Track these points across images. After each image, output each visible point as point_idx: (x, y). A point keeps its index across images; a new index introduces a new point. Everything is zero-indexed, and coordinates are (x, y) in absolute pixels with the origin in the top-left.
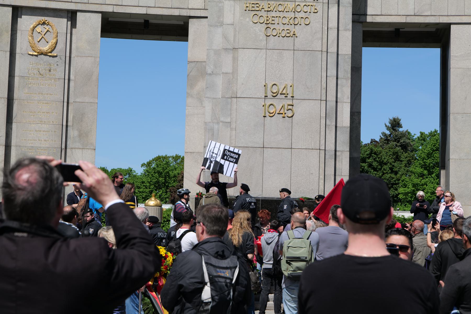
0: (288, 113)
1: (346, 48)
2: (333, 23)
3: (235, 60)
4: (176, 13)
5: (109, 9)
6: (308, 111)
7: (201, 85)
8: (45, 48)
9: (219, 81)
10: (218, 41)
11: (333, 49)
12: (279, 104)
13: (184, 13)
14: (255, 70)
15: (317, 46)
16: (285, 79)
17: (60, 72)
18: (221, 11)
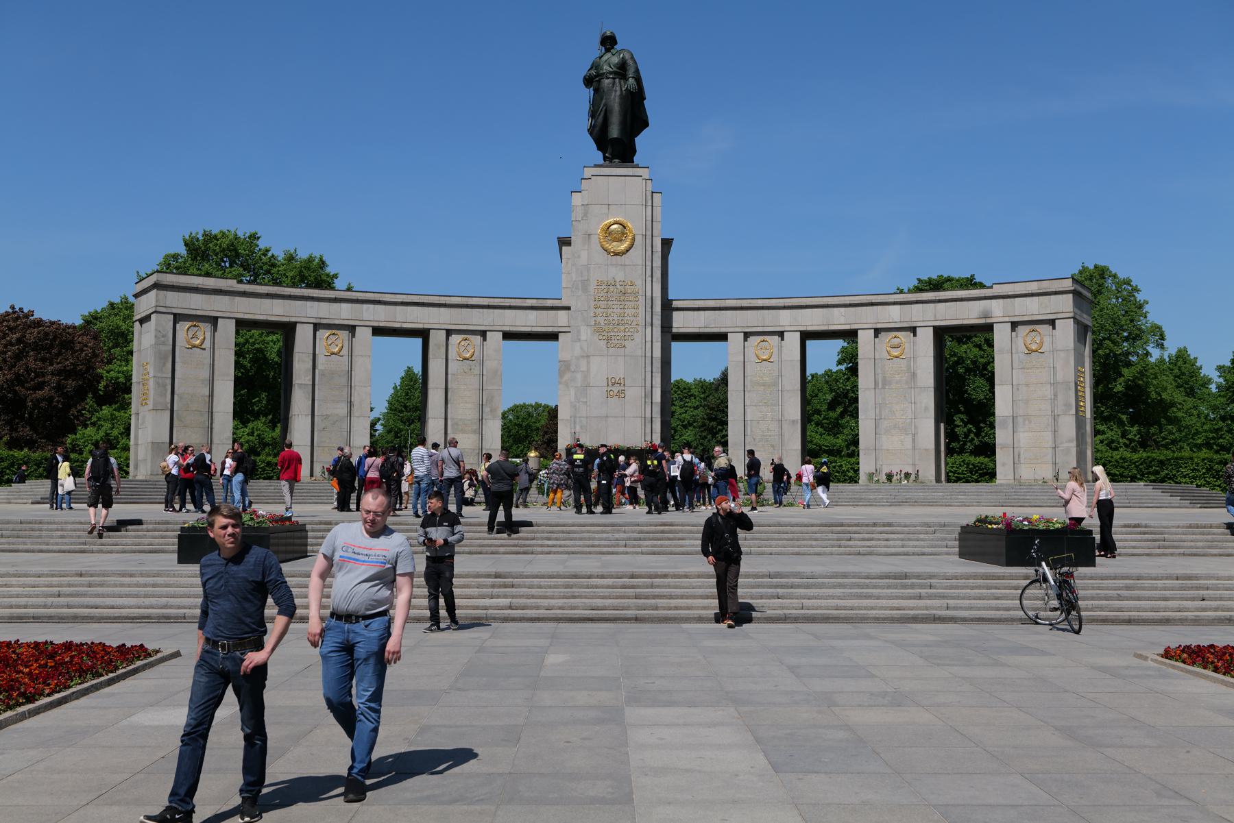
0: (621, 395)
1: (657, 353)
2: (649, 338)
3: (588, 363)
4: (550, 329)
5: (507, 329)
6: (634, 393)
7: (567, 376)
8: (468, 356)
9: (579, 376)
10: (577, 352)
11: (649, 354)
12: (615, 389)
13: (556, 330)
14: (601, 368)
15: (639, 353)
16: (620, 374)
17: (477, 371)
18: (579, 332)
